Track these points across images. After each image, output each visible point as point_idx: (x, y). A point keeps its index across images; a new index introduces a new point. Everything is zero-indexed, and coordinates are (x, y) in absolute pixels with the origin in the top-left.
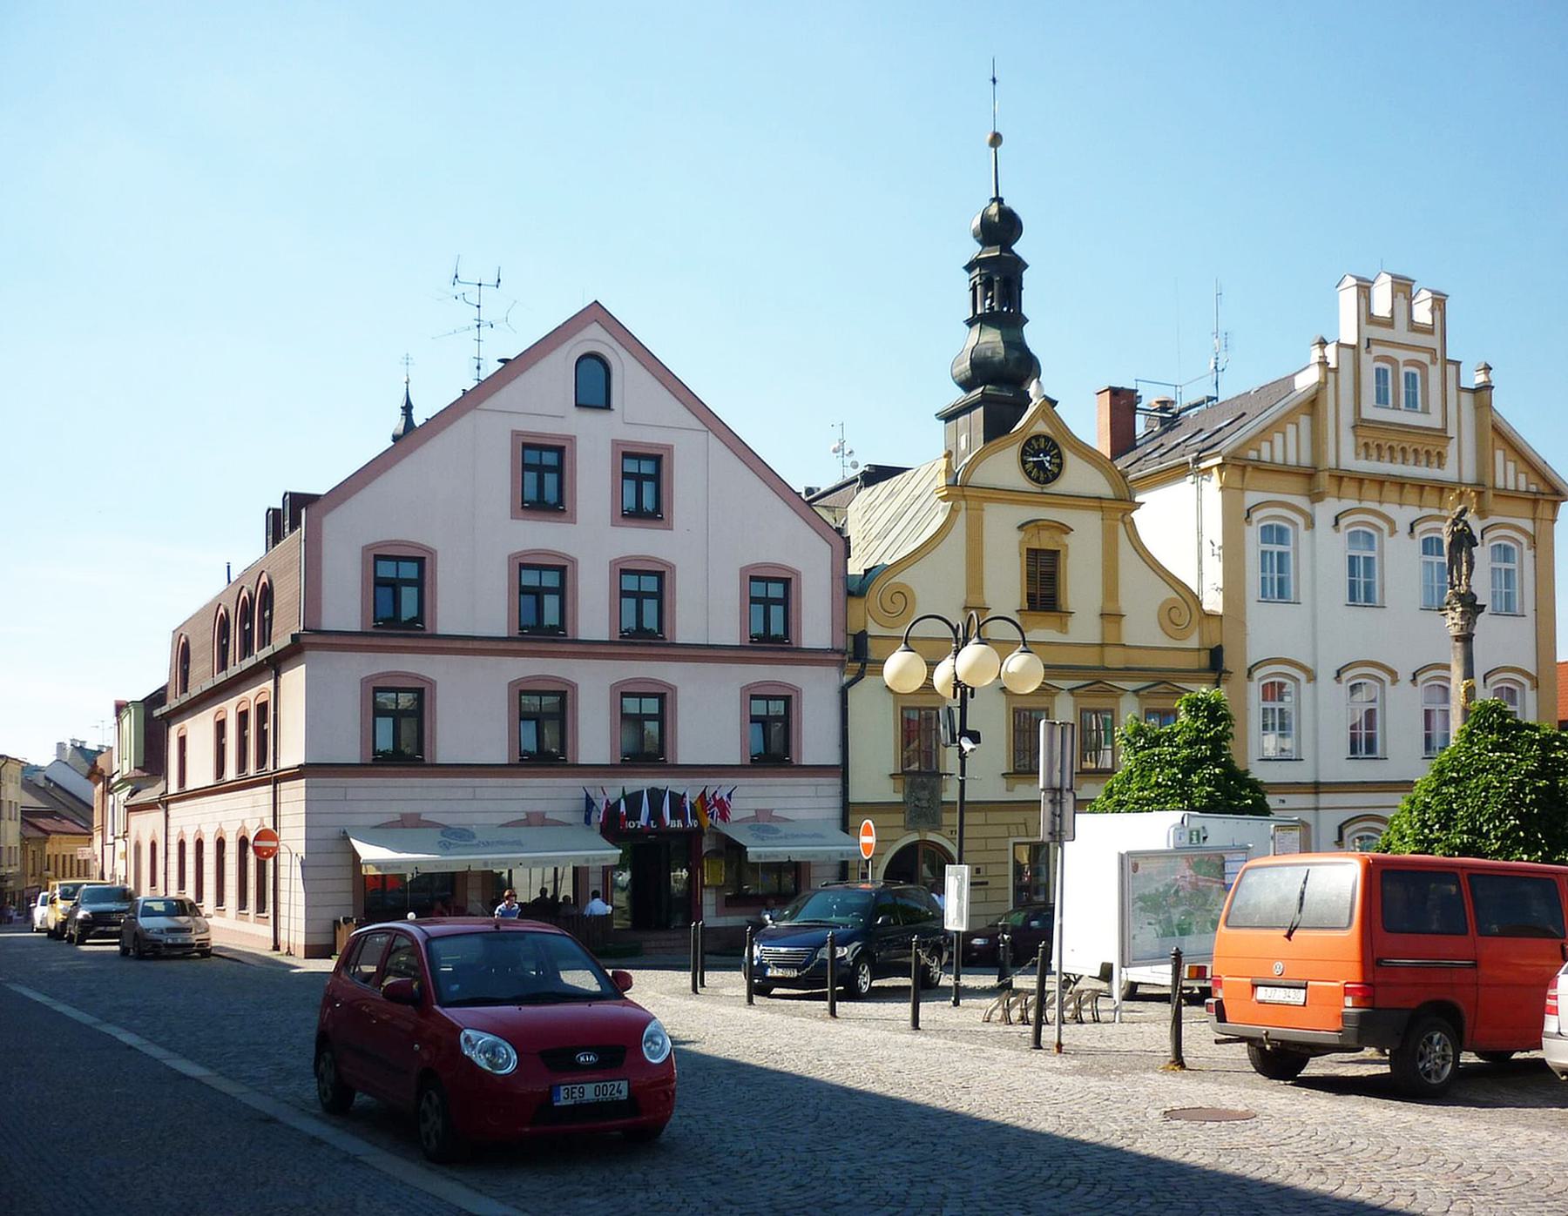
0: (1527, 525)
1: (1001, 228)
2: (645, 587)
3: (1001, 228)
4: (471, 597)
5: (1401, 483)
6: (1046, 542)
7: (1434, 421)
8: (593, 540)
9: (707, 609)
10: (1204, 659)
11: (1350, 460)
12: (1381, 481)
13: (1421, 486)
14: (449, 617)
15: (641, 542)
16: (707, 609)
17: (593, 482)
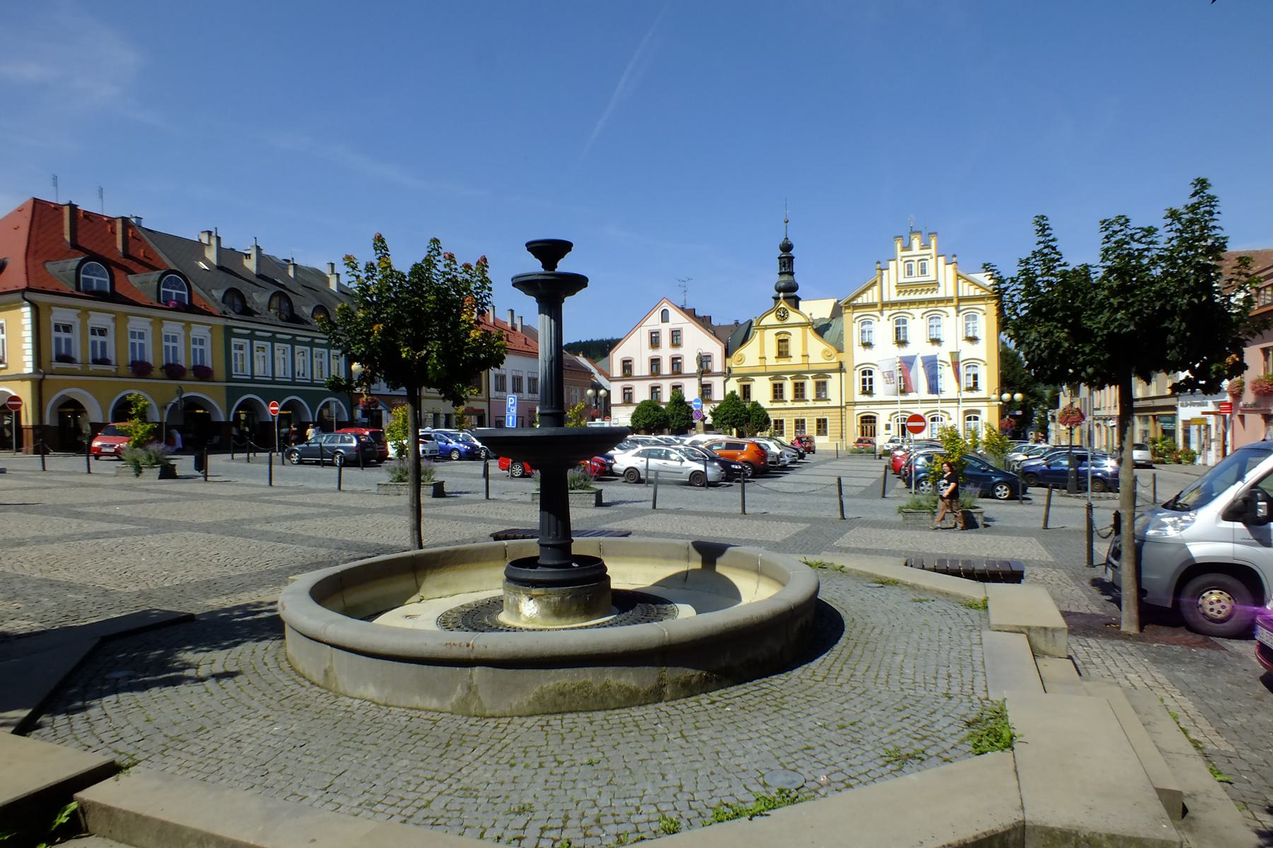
0: (983, 307)
1: (787, 248)
2: (676, 362)
3: (787, 248)
4: (642, 368)
5: (912, 303)
6: (782, 337)
7: (933, 278)
8: (665, 353)
9: (690, 366)
10: (837, 366)
11: (894, 297)
12: (903, 303)
13: (921, 302)
14: (636, 372)
15: (676, 352)
16: (690, 366)
17: (665, 339)
